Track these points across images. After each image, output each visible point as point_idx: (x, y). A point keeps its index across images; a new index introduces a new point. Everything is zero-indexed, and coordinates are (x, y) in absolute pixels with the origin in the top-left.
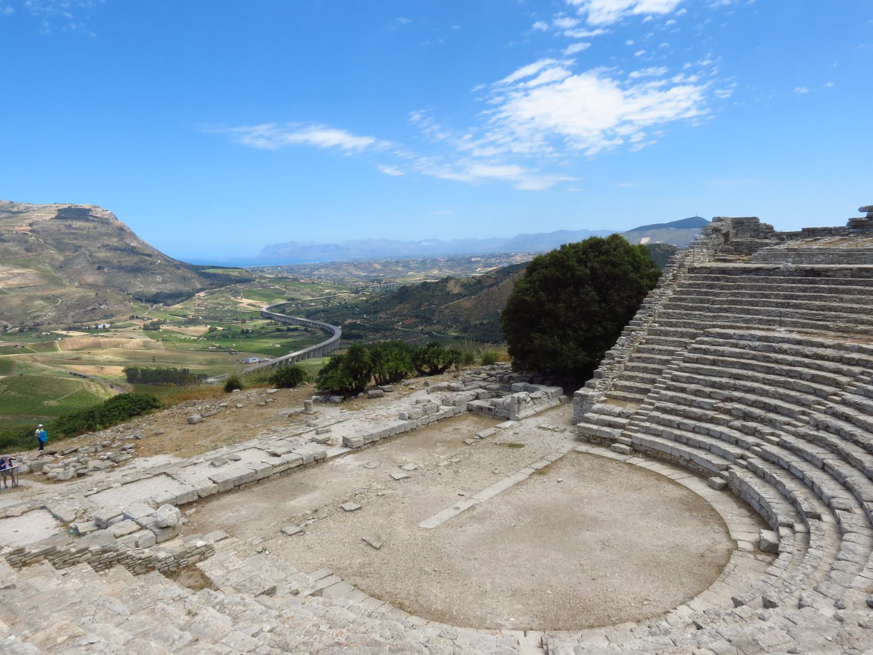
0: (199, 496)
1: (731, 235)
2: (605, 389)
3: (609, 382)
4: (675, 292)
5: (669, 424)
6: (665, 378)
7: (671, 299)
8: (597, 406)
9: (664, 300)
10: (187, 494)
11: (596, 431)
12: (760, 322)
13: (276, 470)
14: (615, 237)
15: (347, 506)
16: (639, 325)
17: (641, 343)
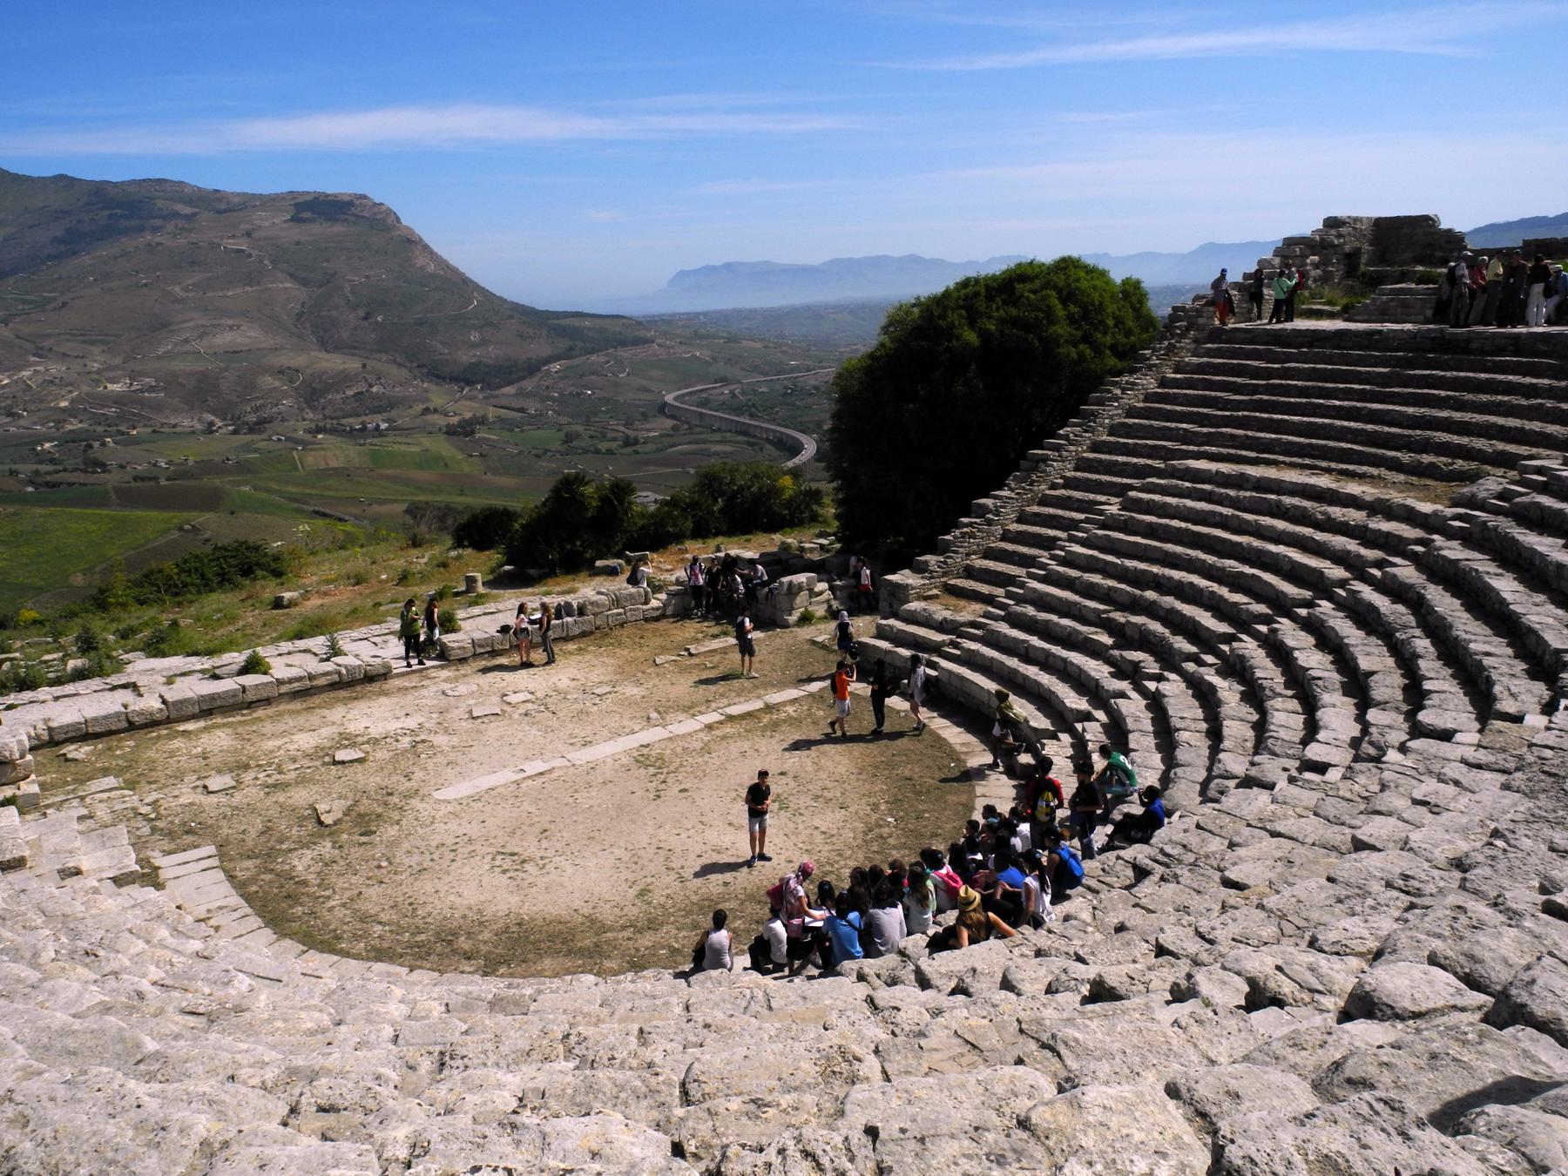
0: (129, 722)
1: (1364, 259)
2: (945, 574)
3: (957, 560)
4: (1163, 383)
5: (1010, 648)
6: (1053, 558)
7: (1149, 398)
8: (915, 605)
9: (1134, 400)
10: (106, 717)
11: (887, 652)
12: (1289, 449)
13: (284, 689)
14: (1067, 265)
15: (341, 755)
16: (1057, 448)
17: (1054, 486)
